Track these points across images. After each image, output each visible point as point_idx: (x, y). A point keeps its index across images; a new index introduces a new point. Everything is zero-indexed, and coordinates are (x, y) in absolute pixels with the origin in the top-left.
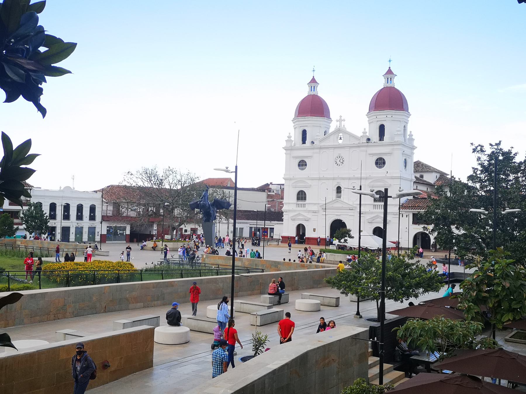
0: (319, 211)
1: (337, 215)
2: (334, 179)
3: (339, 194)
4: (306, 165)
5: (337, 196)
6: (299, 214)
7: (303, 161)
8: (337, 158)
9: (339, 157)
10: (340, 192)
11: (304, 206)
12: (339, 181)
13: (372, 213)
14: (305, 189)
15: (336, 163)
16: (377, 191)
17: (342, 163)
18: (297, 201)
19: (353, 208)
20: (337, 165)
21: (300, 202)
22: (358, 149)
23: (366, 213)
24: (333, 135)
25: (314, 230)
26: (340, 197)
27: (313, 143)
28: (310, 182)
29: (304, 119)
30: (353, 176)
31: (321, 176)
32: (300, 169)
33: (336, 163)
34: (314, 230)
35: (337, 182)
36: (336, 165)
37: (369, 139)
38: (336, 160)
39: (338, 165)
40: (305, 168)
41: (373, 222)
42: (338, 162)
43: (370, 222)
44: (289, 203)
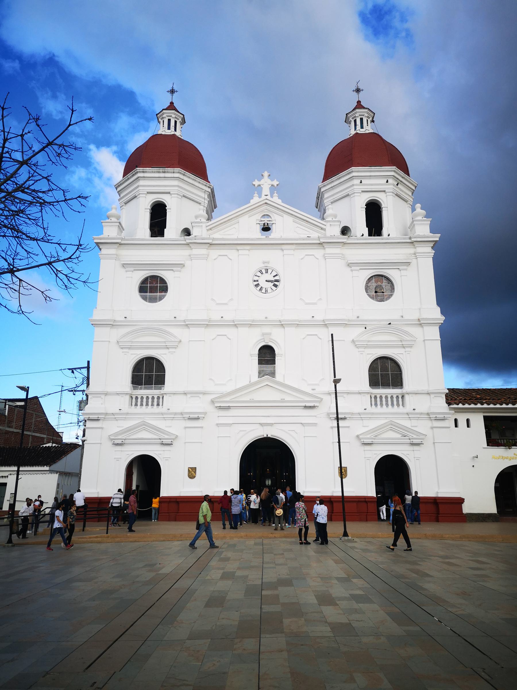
0: (205, 413)
1: (261, 424)
2: (251, 325)
3: (268, 368)
4: (164, 289)
5: (260, 373)
6: (144, 426)
7: (154, 279)
8: (259, 274)
9: (264, 271)
10: (272, 361)
11: (155, 403)
12: (267, 330)
13: (372, 416)
14: (166, 351)
15: (257, 285)
16: (377, 359)
17: (276, 286)
18: (135, 388)
19: (316, 404)
20: (261, 289)
21: (143, 392)
22: (319, 252)
23: (353, 416)
24: (246, 217)
25: (192, 473)
26: (273, 374)
27: (187, 232)
28: (178, 332)
29: (162, 175)
30: (310, 318)
31: (215, 316)
32: (145, 298)
33: (257, 285)
34: (192, 473)
35: (263, 334)
36: (256, 291)
37: (345, 231)
38: (256, 278)
39: (264, 291)
40: (161, 299)
41: (375, 441)
42: (262, 283)
43: (369, 441)
44: (106, 394)
